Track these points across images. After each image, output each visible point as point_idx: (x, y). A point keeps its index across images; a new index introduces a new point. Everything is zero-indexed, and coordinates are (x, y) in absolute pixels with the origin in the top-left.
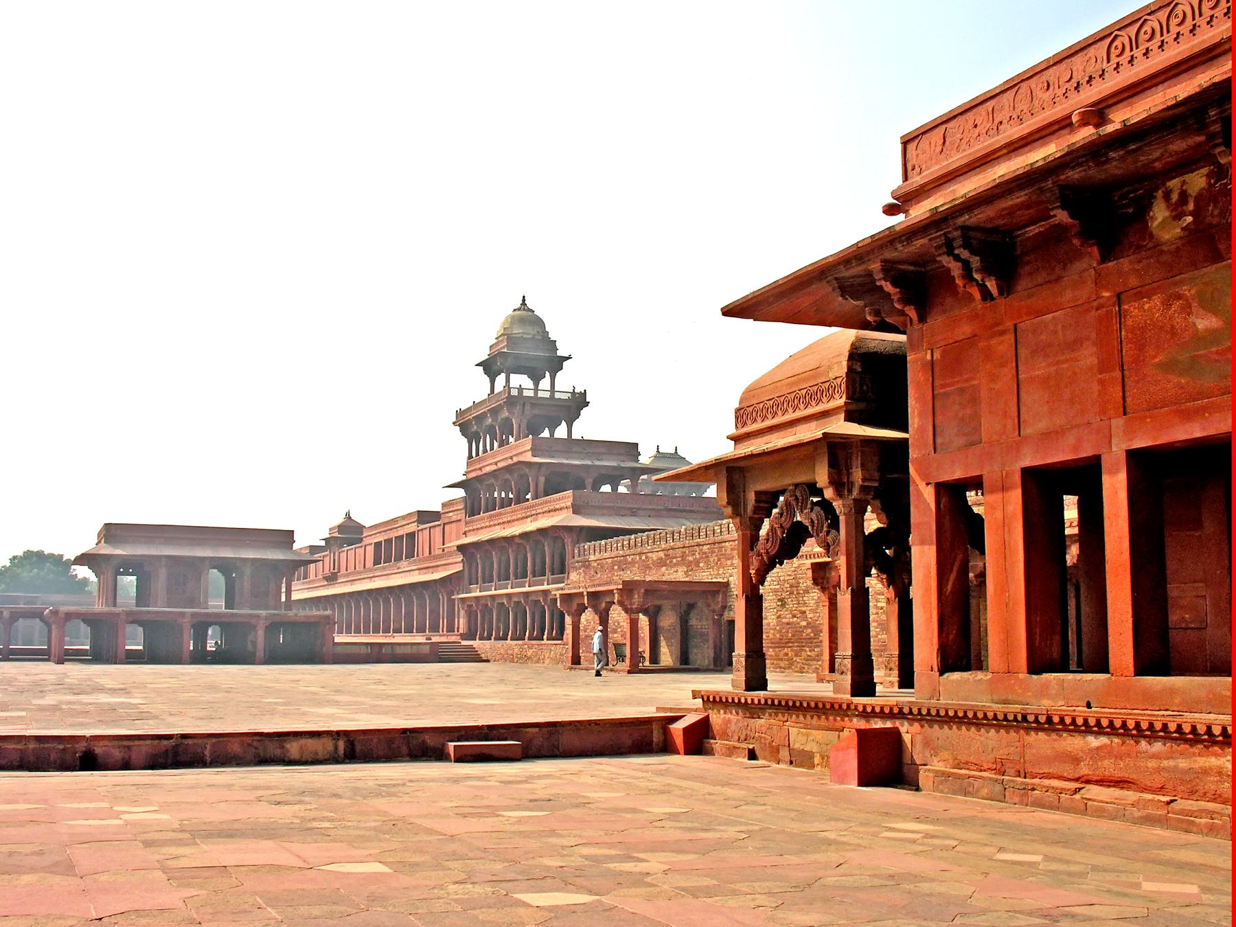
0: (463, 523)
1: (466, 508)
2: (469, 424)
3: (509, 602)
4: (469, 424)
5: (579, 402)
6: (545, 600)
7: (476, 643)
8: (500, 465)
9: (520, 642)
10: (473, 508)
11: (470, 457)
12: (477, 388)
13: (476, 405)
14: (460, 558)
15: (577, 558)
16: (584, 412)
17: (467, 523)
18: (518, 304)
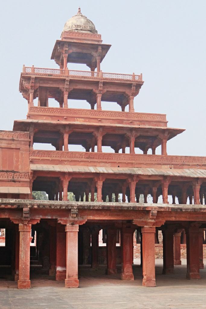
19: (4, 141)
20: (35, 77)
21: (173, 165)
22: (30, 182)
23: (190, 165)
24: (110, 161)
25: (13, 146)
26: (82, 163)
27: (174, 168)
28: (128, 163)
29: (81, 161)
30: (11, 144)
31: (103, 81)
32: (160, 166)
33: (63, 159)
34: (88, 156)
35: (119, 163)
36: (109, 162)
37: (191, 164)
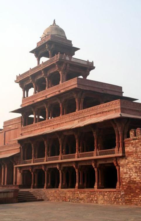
0: (20, 130)
1: (22, 122)
2: (24, 82)
3: (60, 167)
4: (24, 82)
5: (88, 67)
6: (95, 165)
7: (31, 190)
8: (48, 97)
9: (73, 190)
10: (26, 121)
11: (24, 97)
12: (31, 63)
13: (31, 70)
14: (19, 146)
15: (131, 137)
16: (91, 72)
17: (22, 129)
18: (52, 23)
19: (14, 125)
20: (19, 81)
21: (80, 119)
22: (20, 148)
23: (89, 116)
24: (50, 125)
25: (16, 127)
26: (39, 130)
27: (81, 121)
28: (57, 125)
29: (38, 129)
30: (15, 126)
31: (42, 69)
32: (73, 121)
33: (32, 130)
34: (41, 125)
35: (53, 126)
36: (49, 127)
37: (89, 115)
